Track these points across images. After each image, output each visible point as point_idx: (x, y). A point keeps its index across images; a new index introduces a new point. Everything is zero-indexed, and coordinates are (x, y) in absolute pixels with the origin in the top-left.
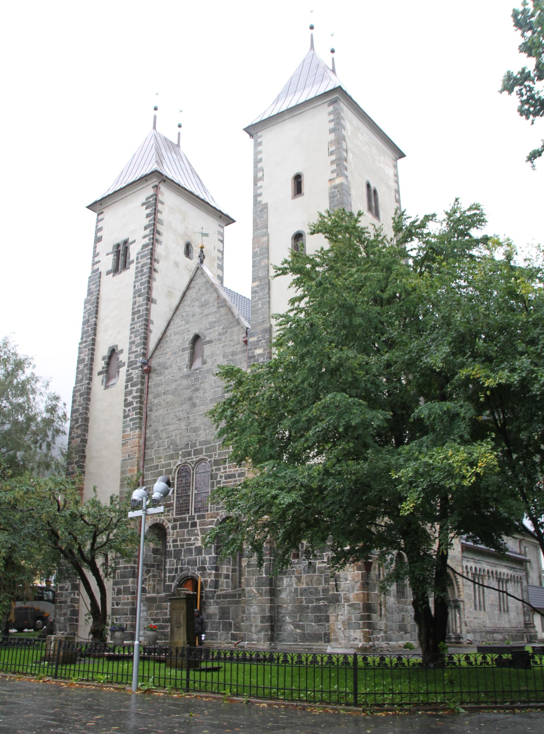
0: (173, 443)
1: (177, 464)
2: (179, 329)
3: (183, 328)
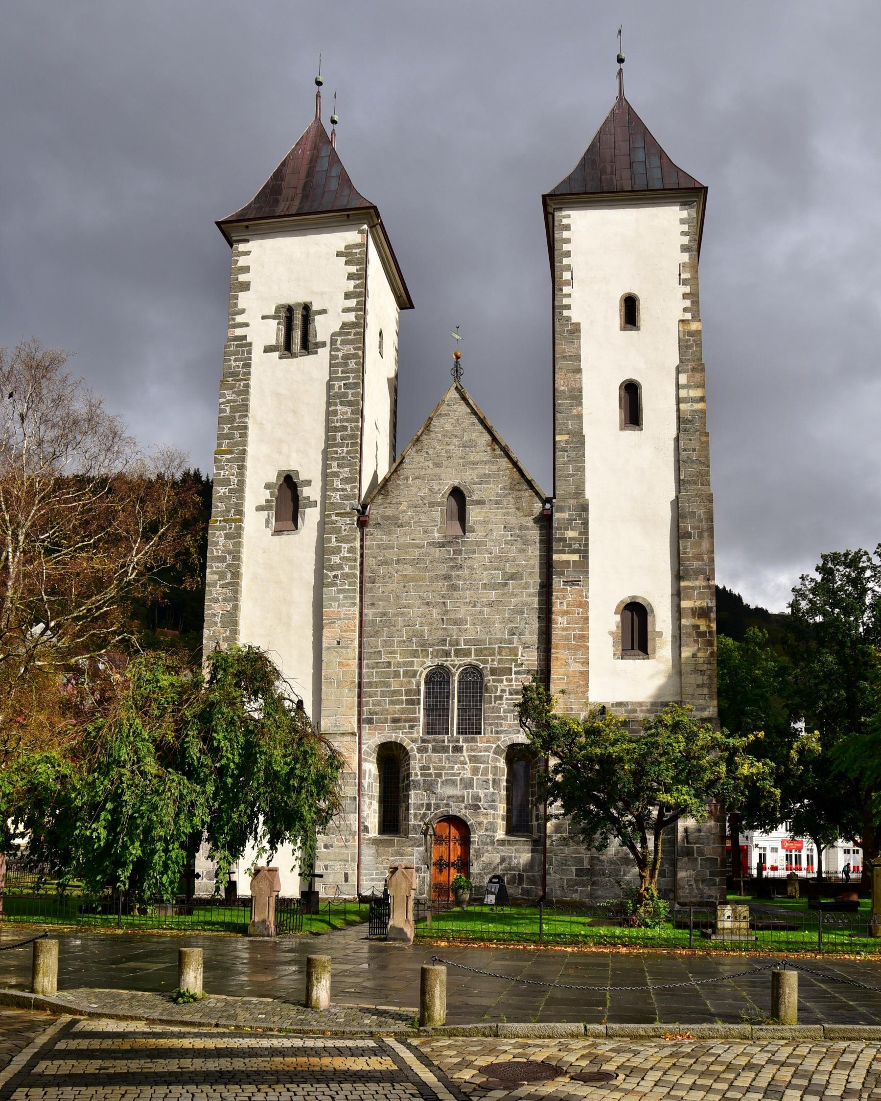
0: (419, 635)
1: (425, 666)
3: (429, 471)
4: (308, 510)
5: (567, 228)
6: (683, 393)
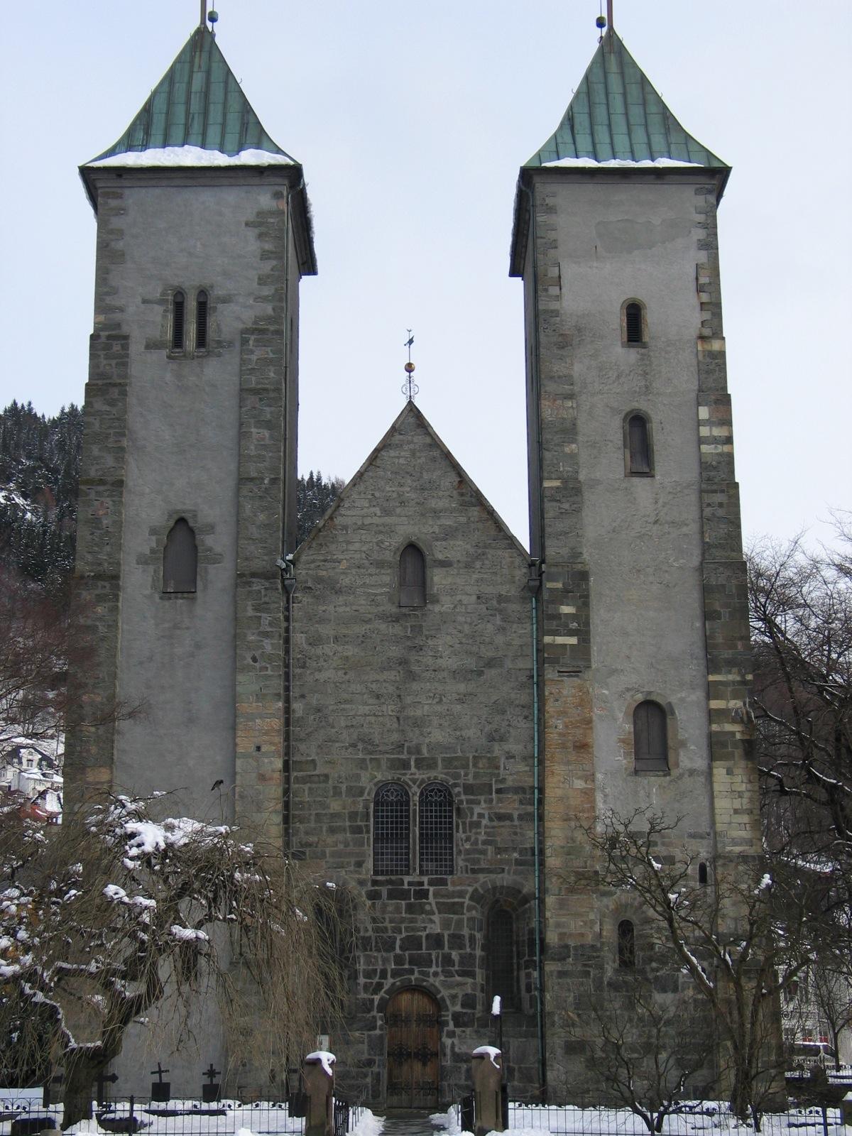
2: (367, 521)
4: (212, 569)
5: (551, 210)
6: (704, 431)
